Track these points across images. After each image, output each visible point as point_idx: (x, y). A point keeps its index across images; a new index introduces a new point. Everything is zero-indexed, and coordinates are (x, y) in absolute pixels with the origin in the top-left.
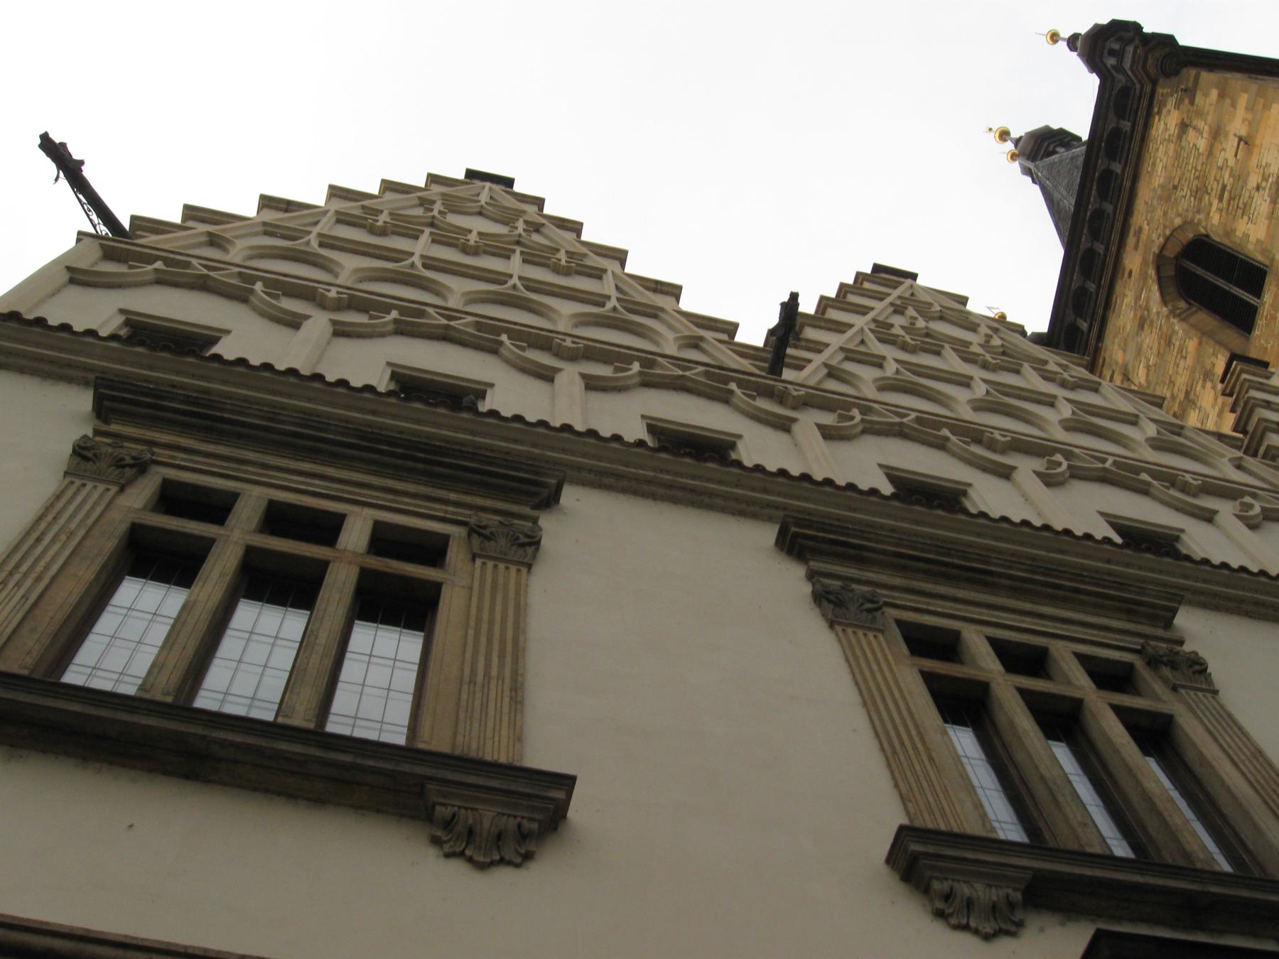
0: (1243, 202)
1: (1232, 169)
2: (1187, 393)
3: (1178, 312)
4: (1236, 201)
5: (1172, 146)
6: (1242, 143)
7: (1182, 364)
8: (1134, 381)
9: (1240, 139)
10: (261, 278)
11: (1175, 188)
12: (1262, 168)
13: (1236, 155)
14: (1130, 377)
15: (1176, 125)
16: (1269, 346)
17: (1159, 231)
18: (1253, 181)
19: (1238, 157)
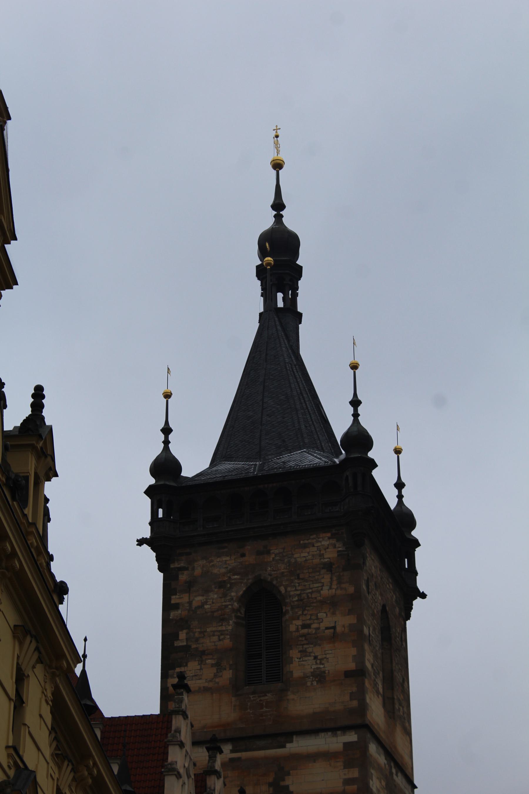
0: (306, 648)
1: (318, 628)
2: (203, 653)
3: (239, 614)
4: (305, 642)
5: (316, 561)
6: (332, 630)
7: (215, 638)
9: (334, 628)
10: (45, 443)
11: (299, 578)
12: (324, 656)
13: (327, 628)
15: (329, 558)
16: (249, 710)
17: (273, 573)
18: (317, 651)
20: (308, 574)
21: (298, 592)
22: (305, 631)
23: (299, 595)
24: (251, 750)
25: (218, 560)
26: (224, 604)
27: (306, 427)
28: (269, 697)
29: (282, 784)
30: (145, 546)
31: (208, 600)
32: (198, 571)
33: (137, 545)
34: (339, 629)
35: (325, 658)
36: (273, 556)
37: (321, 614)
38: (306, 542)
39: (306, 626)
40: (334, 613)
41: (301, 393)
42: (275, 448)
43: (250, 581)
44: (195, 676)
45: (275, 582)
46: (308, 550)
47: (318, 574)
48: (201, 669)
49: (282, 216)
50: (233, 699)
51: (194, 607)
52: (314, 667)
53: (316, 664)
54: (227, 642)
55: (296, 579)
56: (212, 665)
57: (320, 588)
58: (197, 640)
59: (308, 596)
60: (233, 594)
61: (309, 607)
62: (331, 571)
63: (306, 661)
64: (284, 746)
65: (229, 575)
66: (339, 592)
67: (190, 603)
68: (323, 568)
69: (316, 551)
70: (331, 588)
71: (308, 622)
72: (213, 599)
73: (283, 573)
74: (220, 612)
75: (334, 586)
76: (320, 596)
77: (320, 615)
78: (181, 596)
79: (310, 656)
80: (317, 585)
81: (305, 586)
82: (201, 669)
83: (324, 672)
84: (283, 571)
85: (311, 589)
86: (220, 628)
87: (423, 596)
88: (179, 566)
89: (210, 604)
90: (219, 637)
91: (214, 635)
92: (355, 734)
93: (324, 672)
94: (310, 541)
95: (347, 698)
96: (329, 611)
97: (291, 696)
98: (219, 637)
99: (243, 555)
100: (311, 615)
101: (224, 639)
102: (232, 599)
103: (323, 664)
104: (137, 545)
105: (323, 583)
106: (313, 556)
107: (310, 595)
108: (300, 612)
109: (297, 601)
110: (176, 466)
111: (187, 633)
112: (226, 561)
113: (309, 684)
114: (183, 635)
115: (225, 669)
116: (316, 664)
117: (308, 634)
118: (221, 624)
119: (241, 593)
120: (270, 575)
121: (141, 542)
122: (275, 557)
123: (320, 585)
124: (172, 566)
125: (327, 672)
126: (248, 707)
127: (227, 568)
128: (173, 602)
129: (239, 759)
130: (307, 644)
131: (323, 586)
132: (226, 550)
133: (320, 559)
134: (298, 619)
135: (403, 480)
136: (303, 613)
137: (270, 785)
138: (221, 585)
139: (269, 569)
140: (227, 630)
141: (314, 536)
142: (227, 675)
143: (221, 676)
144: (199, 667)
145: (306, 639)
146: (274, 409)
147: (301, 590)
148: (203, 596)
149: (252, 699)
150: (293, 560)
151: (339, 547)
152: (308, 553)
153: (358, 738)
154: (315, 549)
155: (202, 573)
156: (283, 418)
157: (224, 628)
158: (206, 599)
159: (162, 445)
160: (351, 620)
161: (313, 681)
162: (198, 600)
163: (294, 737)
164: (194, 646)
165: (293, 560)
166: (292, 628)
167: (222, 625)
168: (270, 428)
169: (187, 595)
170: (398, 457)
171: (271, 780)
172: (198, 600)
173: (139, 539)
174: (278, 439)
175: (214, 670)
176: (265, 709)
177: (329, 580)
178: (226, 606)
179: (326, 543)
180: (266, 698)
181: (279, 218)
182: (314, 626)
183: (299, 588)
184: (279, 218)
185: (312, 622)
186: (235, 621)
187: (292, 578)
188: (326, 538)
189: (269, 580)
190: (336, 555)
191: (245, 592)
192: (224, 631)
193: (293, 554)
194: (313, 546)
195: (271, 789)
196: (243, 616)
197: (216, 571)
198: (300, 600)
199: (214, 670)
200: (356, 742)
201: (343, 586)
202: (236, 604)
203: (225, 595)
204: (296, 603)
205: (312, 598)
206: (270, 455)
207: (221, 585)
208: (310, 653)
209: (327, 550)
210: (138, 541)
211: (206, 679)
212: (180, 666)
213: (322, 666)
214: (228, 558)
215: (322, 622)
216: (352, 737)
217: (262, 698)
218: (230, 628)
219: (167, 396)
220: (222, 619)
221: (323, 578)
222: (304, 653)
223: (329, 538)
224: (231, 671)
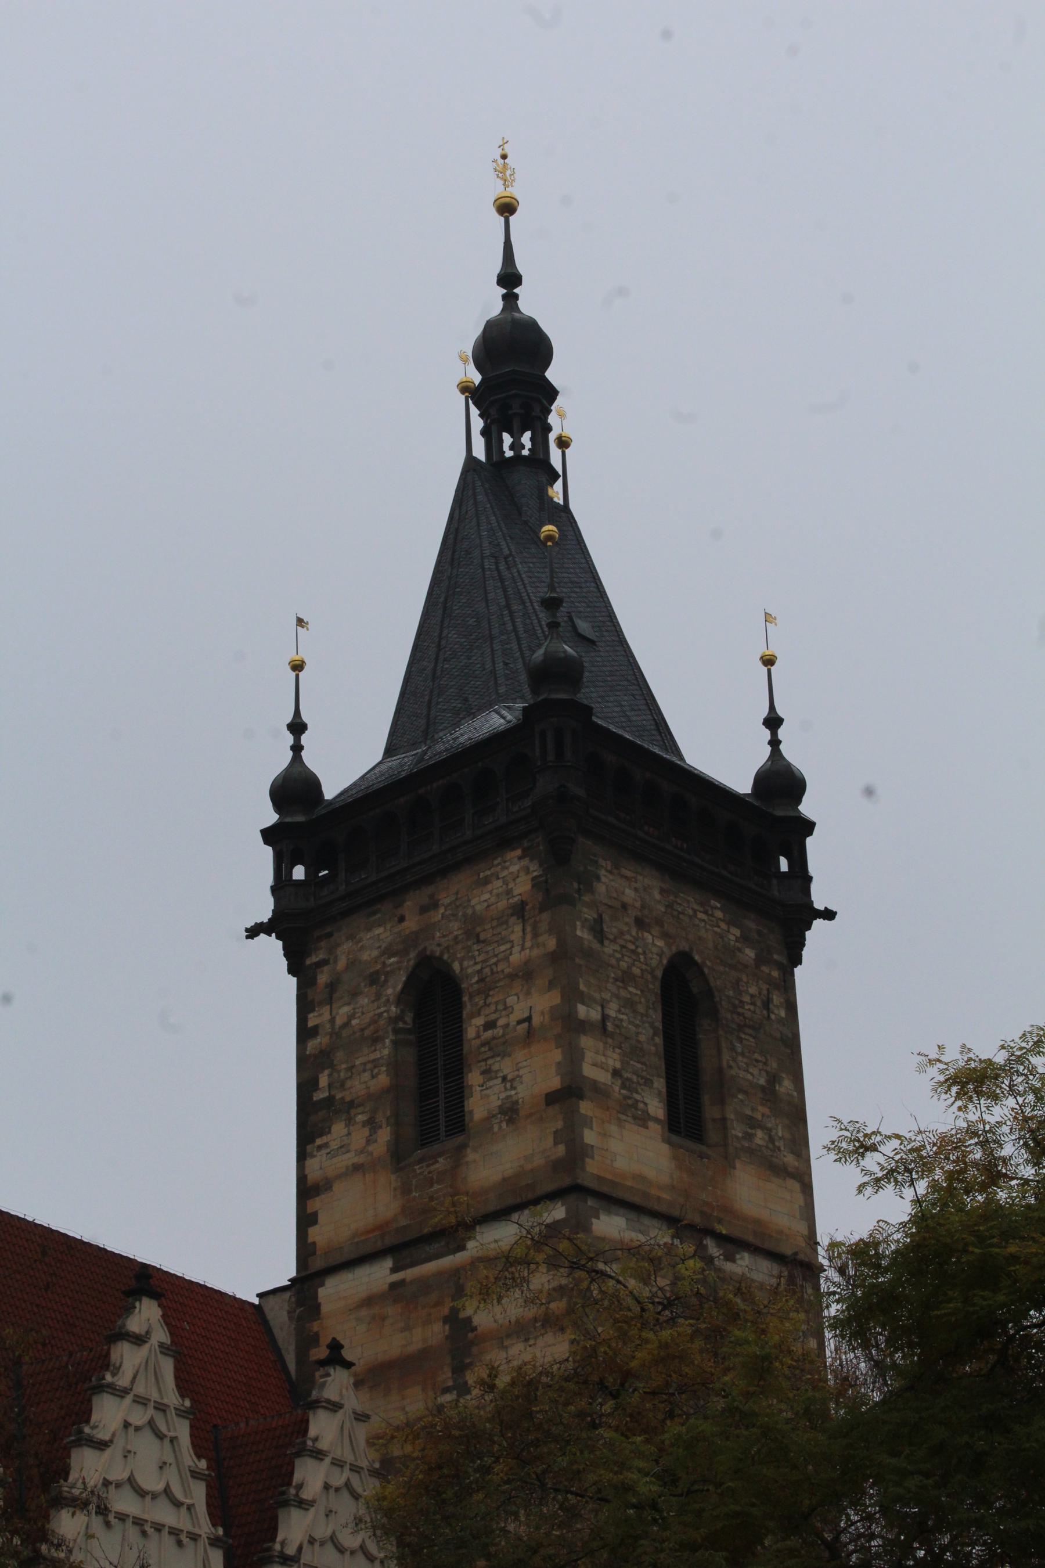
0: (490, 1065)
1: (507, 1025)
2: (352, 1104)
3: (401, 1025)
5: (503, 904)
6: (526, 1025)
7: (366, 1076)
8: (334, 1006)
9: (529, 1019)
11: (478, 941)
12: (517, 1073)
13: (519, 1022)
14: (336, 996)
15: (520, 894)
16: (414, 1194)
18: (505, 1066)
19: (519, 1027)
20: (491, 930)
21: (478, 967)
22: (489, 1034)
23: (479, 972)
24: (413, 1265)
25: (368, 937)
26: (377, 1012)
27: (506, 664)
28: (442, 1164)
29: (462, 1315)
30: (263, 936)
31: (357, 1010)
32: (342, 964)
33: (247, 937)
34: (536, 1020)
35: (518, 1076)
36: (442, 910)
37: (510, 998)
38: (488, 873)
39: (490, 1025)
40: (528, 993)
41: (508, 606)
42: (450, 717)
43: (412, 963)
44: (341, 1147)
45: (446, 957)
46: (490, 887)
47: (505, 926)
48: (349, 1134)
49: (516, 297)
50: (393, 1177)
51: (337, 1027)
52: (503, 1096)
53: (506, 1089)
54: (383, 1079)
55: (474, 944)
56: (365, 1124)
57: (508, 952)
58: (342, 1085)
59: (492, 970)
60: (390, 991)
61: (494, 989)
62: (523, 917)
63: (491, 1087)
64: (462, 1248)
65: (383, 959)
66: (536, 952)
67: (332, 1020)
68: (512, 915)
69: (501, 887)
70: (523, 949)
71: (493, 1017)
72: (362, 1007)
73: (456, 937)
74: (372, 1027)
75: (528, 944)
76: (509, 967)
77: (511, 1000)
78: (321, 1012)
79: (497, 1078)
80: (503, 948)
81: (487, 952)
82: (349, 1134)
83: (517, 1102)
84: (456, 933)
85: (496, 956)
86: (372, 1057)
87: (829, 915)
88: (317, 959)
89: (359, 1017)
90: (372, 1071)
91: (364, 1071)
92: (562, 1205)
93: (517, 1102)
94: (492, 870)
95: (550, 1140)
96: (522, 990)
97: (471, 1156)
98: (372, 1071)
99: (402, 919)
100: (497, 1003)
101: (378, 1074)
102: (388, 1000)
103: (515, 1088)
104: (247, 937)
105: (512, 941)
106: (498, 895)
107: (494, 967)
108: (481, 1003)
109: (477, 982)
110: (313, 784)
111: (330, 1075)
112: (378, 935)
113: (496, 1128)
114: (324, 1080)
115: (381, 1127)
116: (506, 1089)
117: (494, 1038)
118: (373, 1048)
119: (400, 987)
120: (439, 945)
121: (253, 932)
122: (446, 910)
123: (508, 946)
124: (308, 962)
125: (520, 1101)
126: (413, 1187)
127: (380, 947)
128: (310, 1024)
129: (402, 1283)
130: (492, 1057)
131: (512, 947)
132: (378, 916)
133: (508, 899)
134: (479, 1015)
135: (780, 712)
136: (485, 1002)
137: (446, 1320)
138: (374, 979)
139: (438, 934)
140: (382, 1058)
141: (499, 860)
142: (384, 1135)
143: (376, 1141)
144: (345, 1131)
145: (490, 1050)
146: (456, 646)
147: (483, 961)
148: (349, 1004)
149: (418, 1172)
150: (469, 911)
151: (535, 871)
152: (491, 892)
153: (567, 1212)
154: (500, 883)
155: (347, 964)
156: (469, 659)
157: (377, 1055)
158: (354, 1009)
159: (291, 754)
160: (553, 999)
161: (501, 1122)
162: (345, 1010)
163: (478, 1228)
164: (338, 1096)
165: (469, 911)
166: (471, 1032)
167: (375, 1050)
168: (446, 683)
169: (328, 1007)
170: (769, 671)
171: (446, 1311)
172: (345, 1010)
173: (249, 927)
174: (456, 698)
175: (366, 1131)
176: (436, 1187)
177: (521, 934)
178: (380, 1015)
179: (514, 869)
180: (437, 1165)
181: (510, 300)
182: (501, 1022)
183: (478, 959)
184: (510, 300)
185: (499, 1016)
186: (394, 1038)
187: (469, 943)
188: (516, 859)
189: (438, 954)
190: (529, 887)
191: (407, 985)
192: (378, 1059)
193: (469, 901)
194: (498, 878)
195: (447, 1327)
196: (409, 1026)
197: (365, 956)
198: (481, 980)
199: (366, 1131)
200: (563, 1220)
201: (540, 939)
202: (393, 1009)
203: (378, 996)
204: (476, 986)
205: (497, 972)
206: (442, 730)
207: (374, 979)
208: (497, 1072)
209: (518, 880)
210: (247, 930)
211: (356, 1150)
212: (321, 1135)
213: (513, 1092)
214: (380, 930)
215: (512, 1013)
216: (558, 1212)
217: (432, 1168)
218: (386, 1052)
219: (298, 667)
220: (376, 1040)
221: (513, 932)
222: (488, 1073)
223: (520, 858)
224: (389, 1128)
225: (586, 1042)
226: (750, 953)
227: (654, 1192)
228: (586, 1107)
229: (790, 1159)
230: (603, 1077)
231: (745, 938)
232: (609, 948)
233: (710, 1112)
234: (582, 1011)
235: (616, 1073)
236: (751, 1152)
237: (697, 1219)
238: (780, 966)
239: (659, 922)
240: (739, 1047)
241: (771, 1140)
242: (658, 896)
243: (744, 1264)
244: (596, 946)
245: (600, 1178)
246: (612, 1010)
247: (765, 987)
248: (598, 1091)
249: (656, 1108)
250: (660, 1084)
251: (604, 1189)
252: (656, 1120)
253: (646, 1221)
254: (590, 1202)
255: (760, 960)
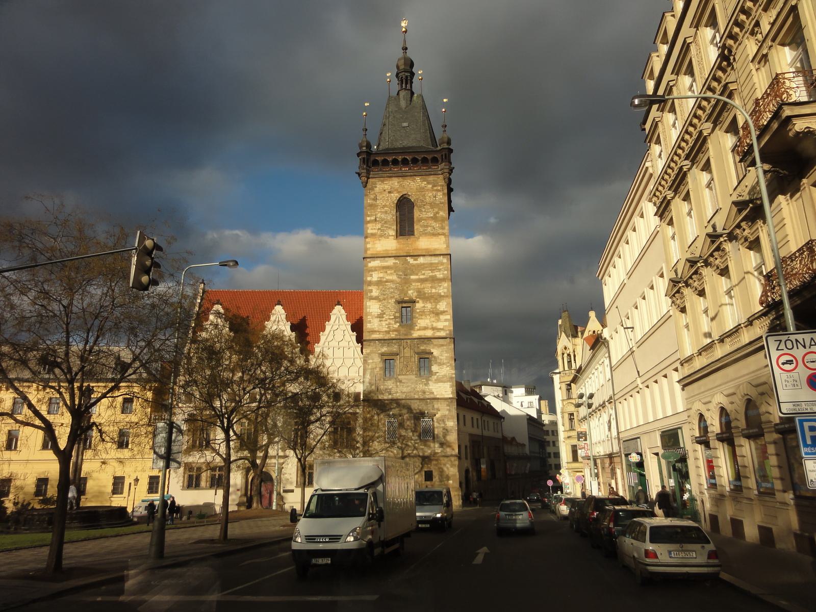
225: (369, 225)
226: (431, 186)
227: (390, 252)
228: (368, 240)
229: (440, 231)
230: (374, 231)
231: (428, 183)
232: (378, 202)
233: (416, 227)
234: (368, 219)
235: (379, 229)
236: (426, 233)
237: (405, 254)
238: (440, 185)
239: (396, 190)
240: (424, 210)
241: (434, 228)
242: (396, 184)
243: (421, 260)
244: (374, 202)
245: (372, 254)
246: (379, 215)
247: (434, 193)
248: (373, 235)
249: (392, 233)
250: (394, 227)
251: (373, 256)
252: (392, 236)
253: (386, 259)
254: (368, 260)
255: (434, 186)
